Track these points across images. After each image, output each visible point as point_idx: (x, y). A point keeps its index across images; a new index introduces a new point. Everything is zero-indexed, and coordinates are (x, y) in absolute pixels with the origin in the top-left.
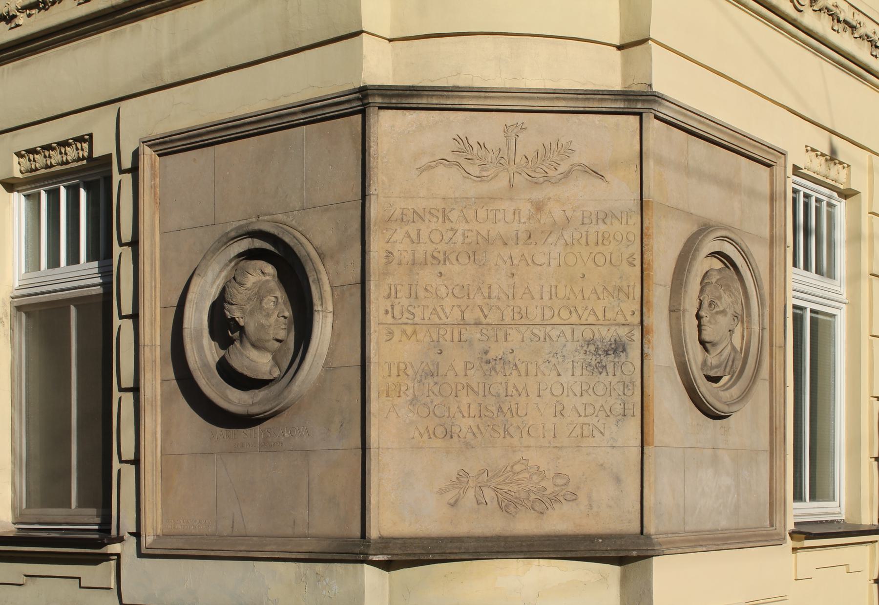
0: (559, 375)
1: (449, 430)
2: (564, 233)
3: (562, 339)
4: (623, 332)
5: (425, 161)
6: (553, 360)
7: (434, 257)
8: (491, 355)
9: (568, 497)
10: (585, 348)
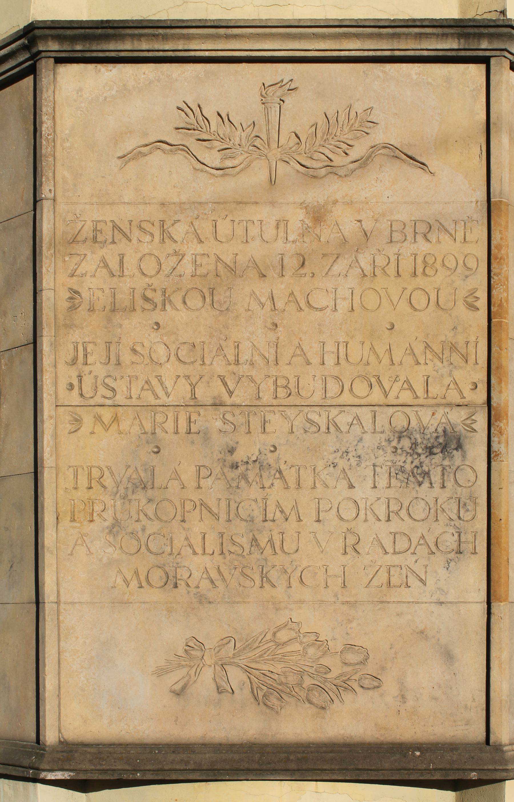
0: (351, 486)
1: (171, 574)
3: (357, 429)
4: (457, 417)
6: (342, 463)
8: (240, 455)
10: (394, 443)
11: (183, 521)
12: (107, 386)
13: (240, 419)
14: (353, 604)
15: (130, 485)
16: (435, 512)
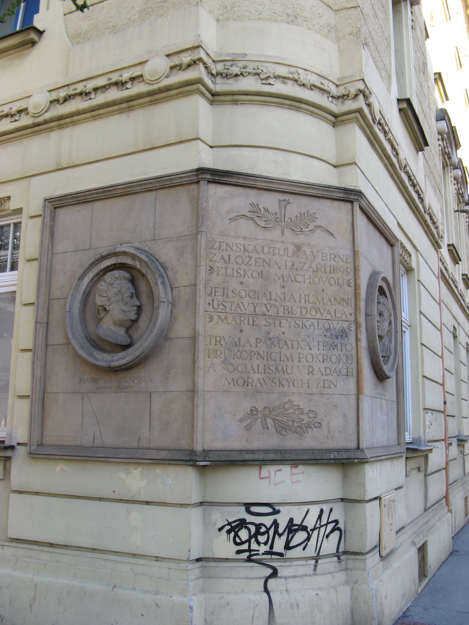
0: (311, 349)
1: (246, 381)
2: (313, 265)
3: (312, 327)
4: (345, 325)
5: (233, 215)
6: (307, 340)
7: (238, 273)
8: (272, 335)
9: (317, 425)
10: (325, 334)
11: (251, 359)
12: (223, 305)
13: (271, 321)
14: (312, 394)
15: (231, 344)
16: (339, 360)
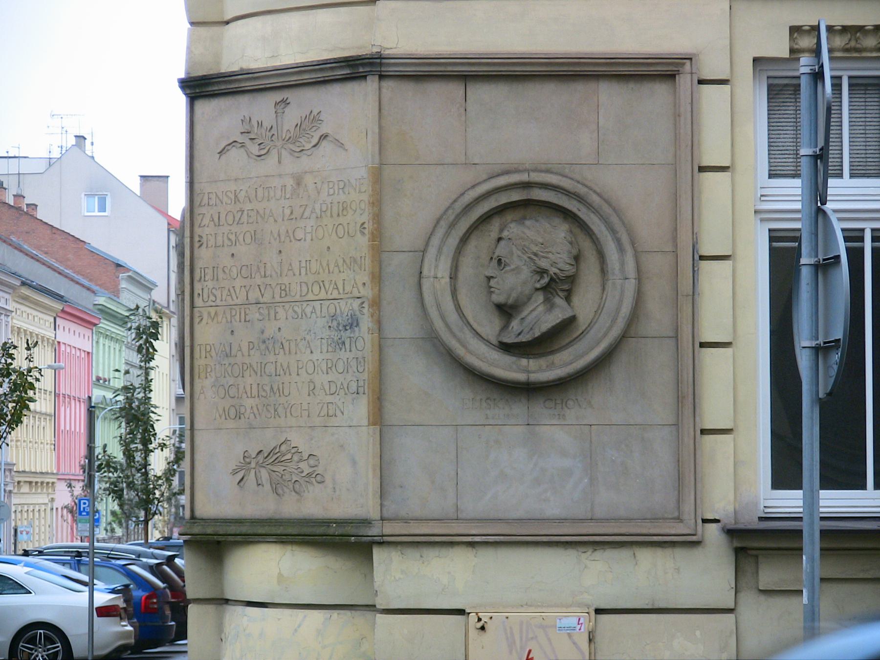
3: (314, 314)
6: (308, 337)
7: (229, 239)
8: (267, 335)
